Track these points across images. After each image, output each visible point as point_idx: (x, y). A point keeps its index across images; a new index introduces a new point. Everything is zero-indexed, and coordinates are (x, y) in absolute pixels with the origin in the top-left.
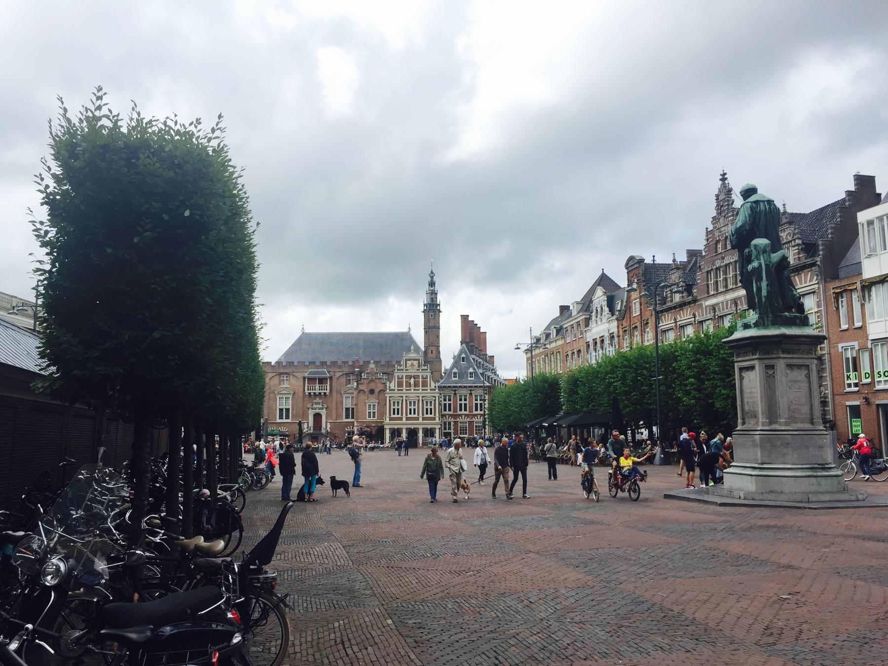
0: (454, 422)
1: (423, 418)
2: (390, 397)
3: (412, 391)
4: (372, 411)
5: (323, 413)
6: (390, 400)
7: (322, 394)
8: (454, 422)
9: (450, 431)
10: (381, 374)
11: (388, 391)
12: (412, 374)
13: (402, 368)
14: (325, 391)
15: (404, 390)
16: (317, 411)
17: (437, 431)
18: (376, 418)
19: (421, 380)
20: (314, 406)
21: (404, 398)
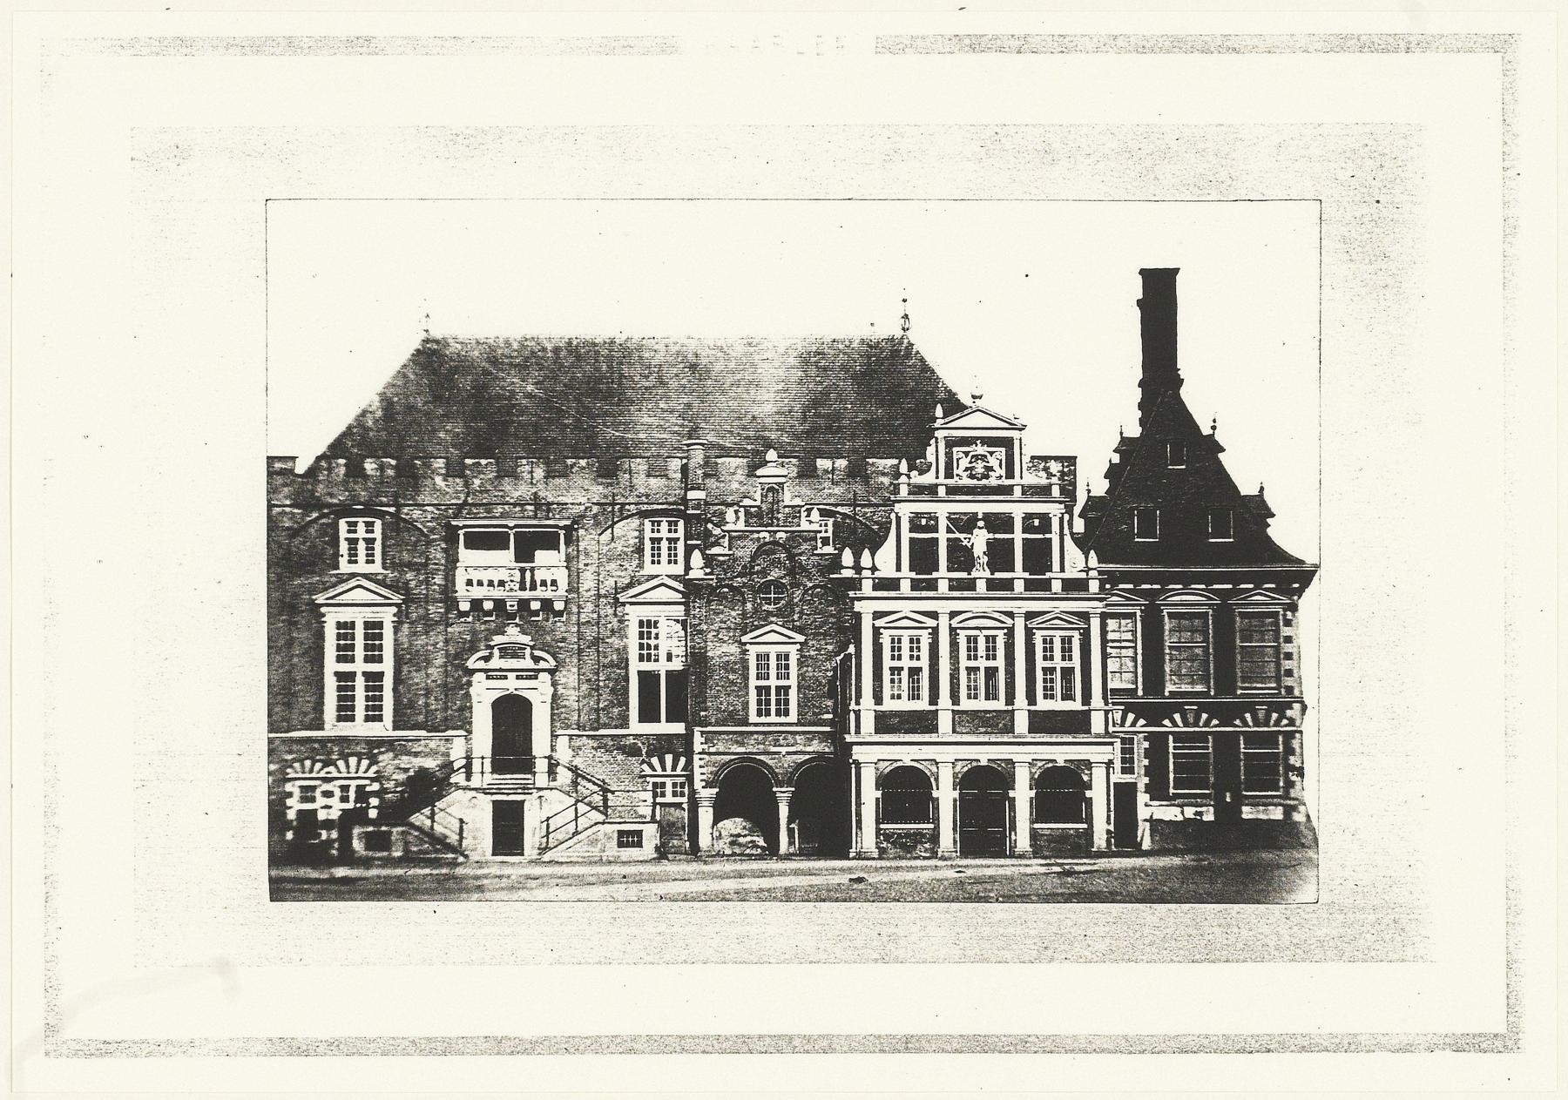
0: (1149, 737)
1: (1033, 715)
2: (877, 615)
3: (981, 586)
4: (773, 682)
5: (539, 695)
6: (876, 632)
7: (535, 606)
8: (1149, 737)
9: (1128, 778)
10: (815, 515)
11: (867, 587)
12: (981, 509)
13: (928, 479)
14: (548, 594)
15: (943, 587)
16: (512, 684)
17: (1099, 774)
18: (793, 716)
19: (1018, 536)
20: (496, 662)
21: (944, 623)
